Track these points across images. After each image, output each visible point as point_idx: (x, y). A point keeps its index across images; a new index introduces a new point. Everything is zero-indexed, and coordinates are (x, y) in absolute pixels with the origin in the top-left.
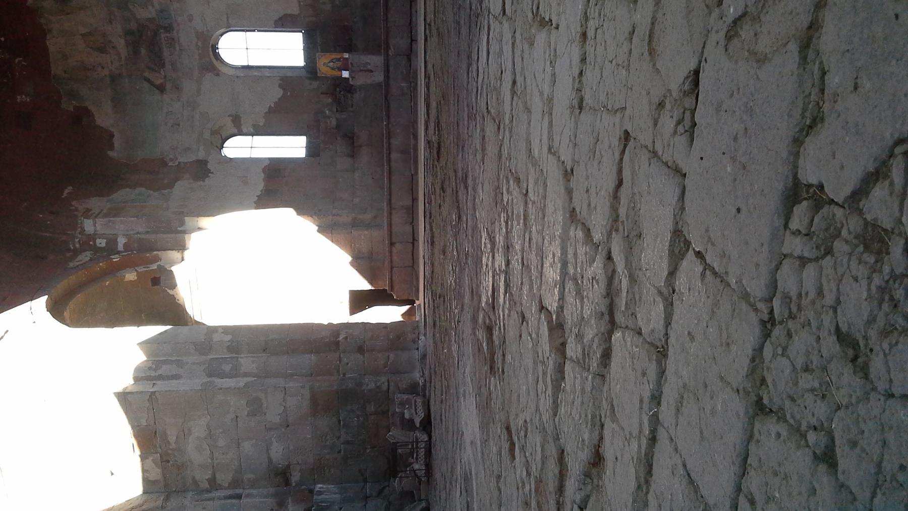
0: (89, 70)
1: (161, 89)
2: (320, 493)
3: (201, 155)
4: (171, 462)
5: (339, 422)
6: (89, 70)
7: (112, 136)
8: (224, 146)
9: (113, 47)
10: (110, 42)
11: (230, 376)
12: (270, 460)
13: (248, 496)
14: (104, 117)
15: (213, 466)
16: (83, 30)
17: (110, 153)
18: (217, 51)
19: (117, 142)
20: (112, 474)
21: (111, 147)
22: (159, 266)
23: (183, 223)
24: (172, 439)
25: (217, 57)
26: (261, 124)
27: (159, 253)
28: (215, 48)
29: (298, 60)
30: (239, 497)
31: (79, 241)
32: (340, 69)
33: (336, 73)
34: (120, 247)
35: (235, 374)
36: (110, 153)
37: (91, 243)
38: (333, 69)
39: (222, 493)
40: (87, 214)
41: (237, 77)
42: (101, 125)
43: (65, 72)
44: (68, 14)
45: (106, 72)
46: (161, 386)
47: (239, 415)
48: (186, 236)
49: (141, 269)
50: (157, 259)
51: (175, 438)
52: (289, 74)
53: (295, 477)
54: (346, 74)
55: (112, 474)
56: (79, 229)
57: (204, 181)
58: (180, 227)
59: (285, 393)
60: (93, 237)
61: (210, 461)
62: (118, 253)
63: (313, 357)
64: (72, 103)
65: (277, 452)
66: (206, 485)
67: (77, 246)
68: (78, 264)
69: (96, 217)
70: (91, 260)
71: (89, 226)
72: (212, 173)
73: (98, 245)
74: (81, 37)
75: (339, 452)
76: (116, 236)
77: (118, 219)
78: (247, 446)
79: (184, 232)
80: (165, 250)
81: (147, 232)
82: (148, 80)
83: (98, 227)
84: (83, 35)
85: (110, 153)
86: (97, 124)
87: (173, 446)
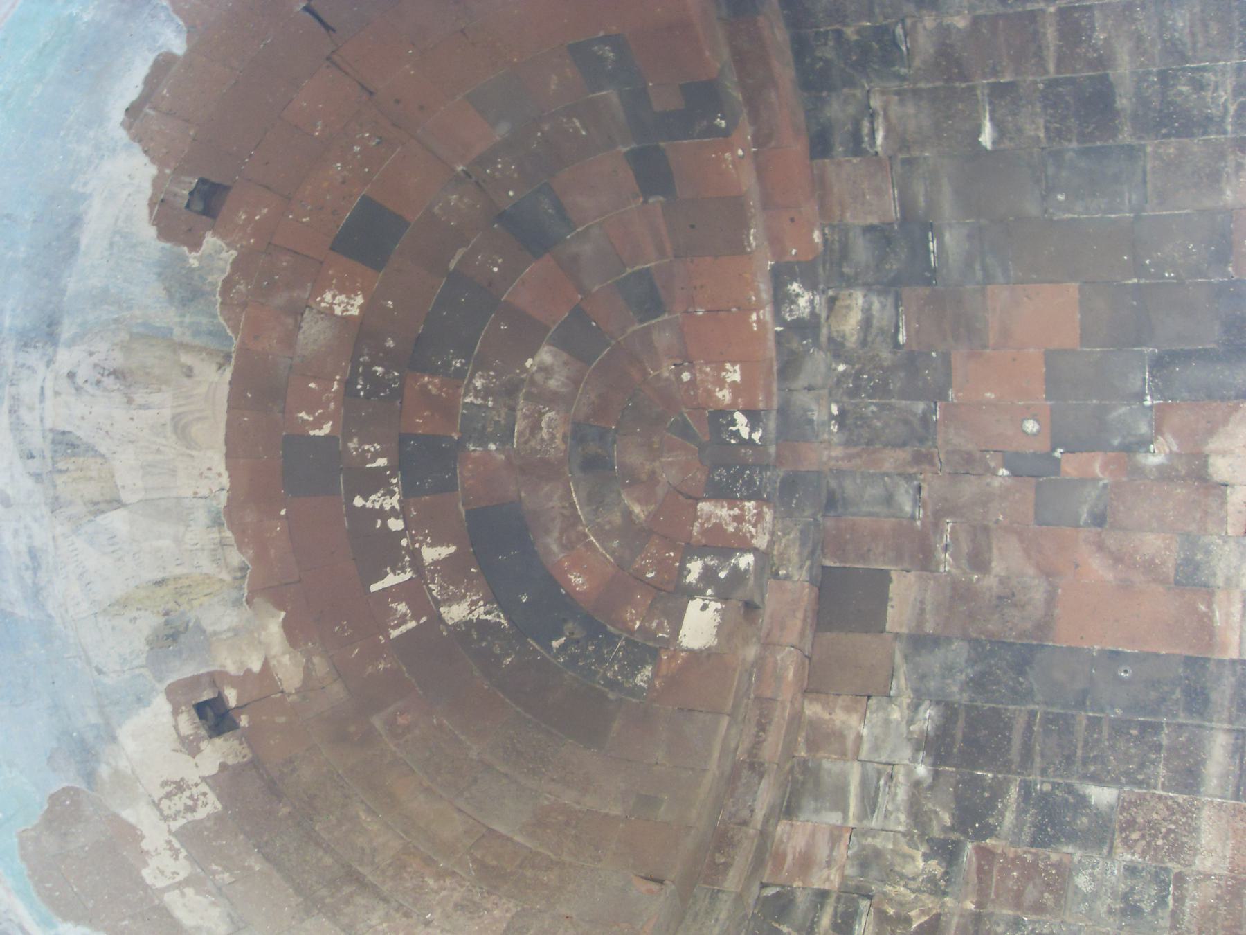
0: (116, 373)
6: (116, 373)
7: (133, 111)
9: (32, 457)
10: (37, 477)
16: (116, 520)
19: (130, 86)
21: (163, 65)
42: (146, 159)
43: (189, 372)
44: (160, 583)
45: (66, 358)
64: (200, 259)
74: (125, 496)
84: (116, 503)
85: (177, 44)
86: (153, 170)
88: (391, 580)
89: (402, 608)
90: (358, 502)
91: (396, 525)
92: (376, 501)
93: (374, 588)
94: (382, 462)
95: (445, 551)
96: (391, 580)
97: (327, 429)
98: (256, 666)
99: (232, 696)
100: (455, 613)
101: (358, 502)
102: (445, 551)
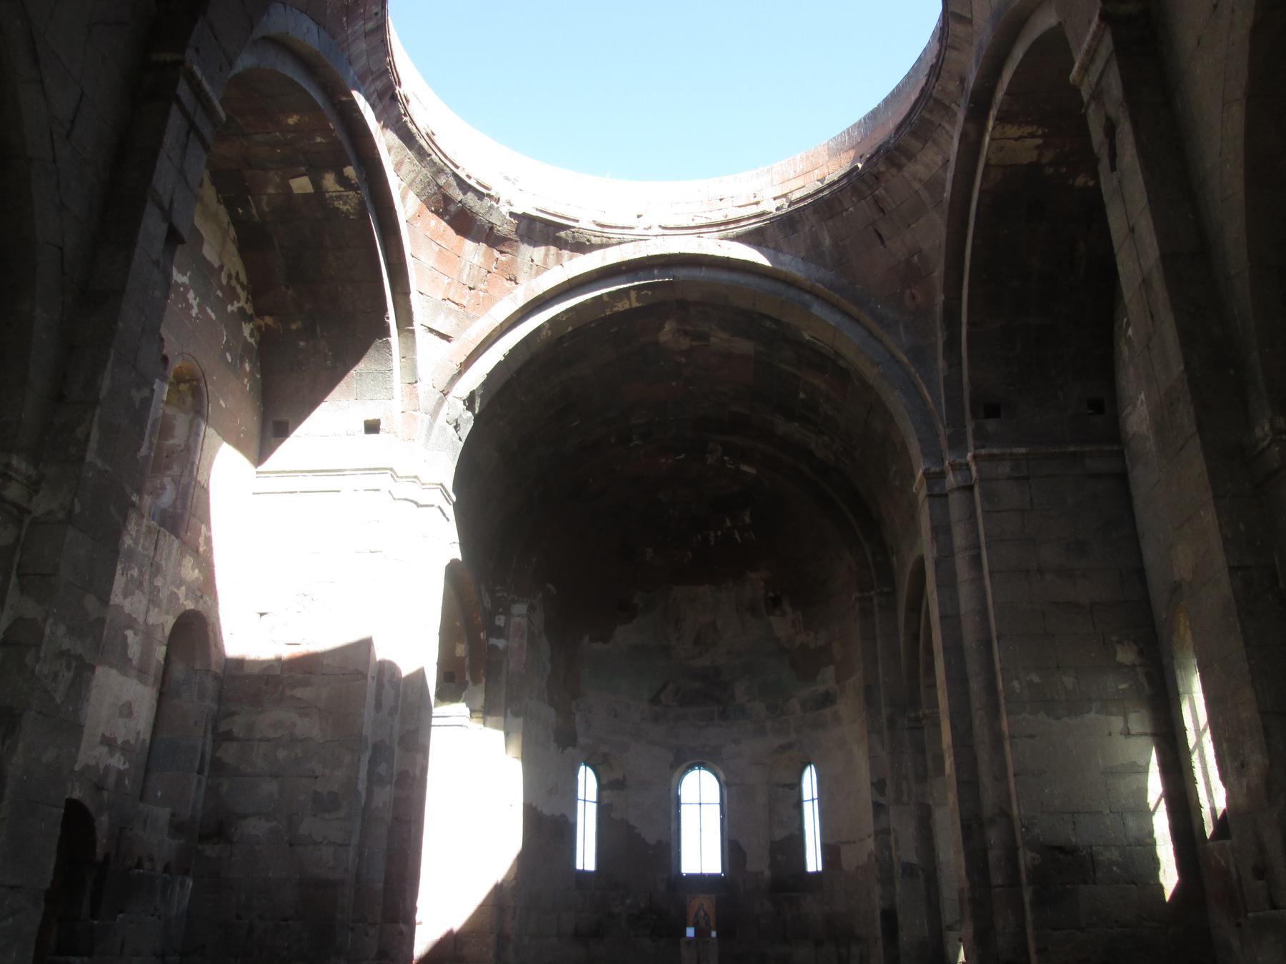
1: (655, 700)
2: (183, 885)
3: (582, 740)
4: (265, 687)
5: (285, 920)
8: (587, 767)
11: (371, 773)
12: (246, 816)
13: (199, 782)
14: (625, 635)
15: (249, 740)
17: (587, 638)
18: (696, 768)
20: (262, 614)
22: (467, 683)
23: (516, 714)
24: (299, 692)
25: (691, 767)
26: (613, 815)
27: (482, 685)
28: (702, 765)
29: (690, 865)
30: (200, 771)
31: (503, 597)
32: (696, 925)
33: (691, 918)
34: (493, 641)
35: (374, 780)
36: (587, 639)
37: (501, 610)
38: (696, 915)
39: (208, 749)
40: (532, 608)
41: (670, 790)
46: (371, 685)
47: (318, 779)
48: (501, 719)
49: (467, 661)
50: (476, 681)
51: (299, 695)
52: (673, 854)
53: (210, 850)
54: (690, 932)
55: (262, 614)
56: (516, 598)
57: (554, 741)
58: (511, 711)
59: (341, 845)
60: (507, 612)
61: (258, 736)
62: (487, 639)
63: (381, 885)
65: (256, 828)
66: (223, 727)
67: (499, 595)
68: (483, 594)
69: (529, 619)
70: (485, 608)
71: (520, 609)
72: (562, 752)
73: (497, 617)
75: (238, 917)
76: (507, 638)
77: (525, 642)
78: (271, 787)
79: (505, 716)
80: (486, 691)
81: (508, 673)
82: (664, 687)
83: (517, 619)
85: (587, 638)
87: (288, 693)
88: (737, 536)
89: (746, 534)
90: (712, 543)
91: (719, 533)
92: (712, 539)
93: (740, 541)
94: (699, 537)
95: (728, 520)
96: (737, 536)
97: (689, 553)
98: (762, 584)
99: (771, 594)
100: (748, 520)
101: (712, 543)
102: (728, 520)
